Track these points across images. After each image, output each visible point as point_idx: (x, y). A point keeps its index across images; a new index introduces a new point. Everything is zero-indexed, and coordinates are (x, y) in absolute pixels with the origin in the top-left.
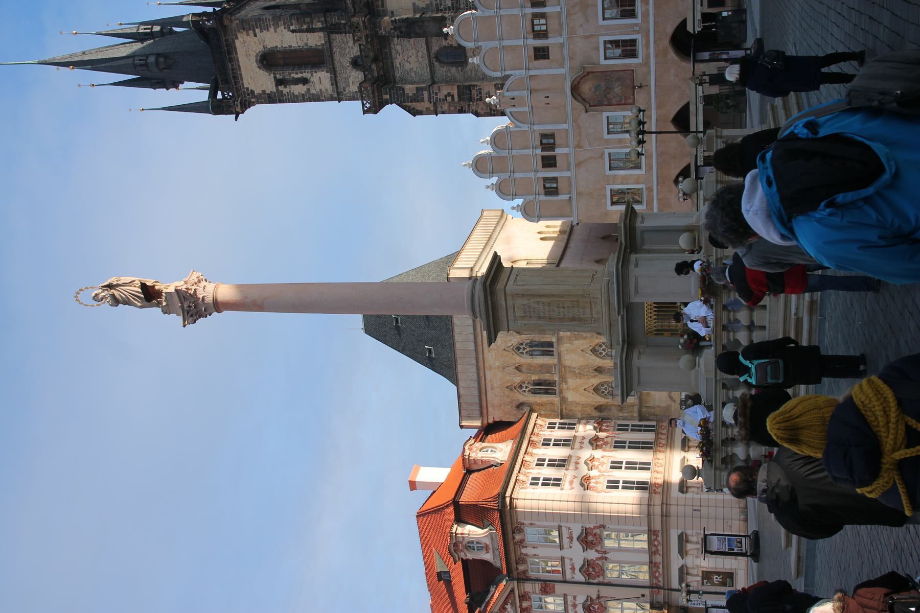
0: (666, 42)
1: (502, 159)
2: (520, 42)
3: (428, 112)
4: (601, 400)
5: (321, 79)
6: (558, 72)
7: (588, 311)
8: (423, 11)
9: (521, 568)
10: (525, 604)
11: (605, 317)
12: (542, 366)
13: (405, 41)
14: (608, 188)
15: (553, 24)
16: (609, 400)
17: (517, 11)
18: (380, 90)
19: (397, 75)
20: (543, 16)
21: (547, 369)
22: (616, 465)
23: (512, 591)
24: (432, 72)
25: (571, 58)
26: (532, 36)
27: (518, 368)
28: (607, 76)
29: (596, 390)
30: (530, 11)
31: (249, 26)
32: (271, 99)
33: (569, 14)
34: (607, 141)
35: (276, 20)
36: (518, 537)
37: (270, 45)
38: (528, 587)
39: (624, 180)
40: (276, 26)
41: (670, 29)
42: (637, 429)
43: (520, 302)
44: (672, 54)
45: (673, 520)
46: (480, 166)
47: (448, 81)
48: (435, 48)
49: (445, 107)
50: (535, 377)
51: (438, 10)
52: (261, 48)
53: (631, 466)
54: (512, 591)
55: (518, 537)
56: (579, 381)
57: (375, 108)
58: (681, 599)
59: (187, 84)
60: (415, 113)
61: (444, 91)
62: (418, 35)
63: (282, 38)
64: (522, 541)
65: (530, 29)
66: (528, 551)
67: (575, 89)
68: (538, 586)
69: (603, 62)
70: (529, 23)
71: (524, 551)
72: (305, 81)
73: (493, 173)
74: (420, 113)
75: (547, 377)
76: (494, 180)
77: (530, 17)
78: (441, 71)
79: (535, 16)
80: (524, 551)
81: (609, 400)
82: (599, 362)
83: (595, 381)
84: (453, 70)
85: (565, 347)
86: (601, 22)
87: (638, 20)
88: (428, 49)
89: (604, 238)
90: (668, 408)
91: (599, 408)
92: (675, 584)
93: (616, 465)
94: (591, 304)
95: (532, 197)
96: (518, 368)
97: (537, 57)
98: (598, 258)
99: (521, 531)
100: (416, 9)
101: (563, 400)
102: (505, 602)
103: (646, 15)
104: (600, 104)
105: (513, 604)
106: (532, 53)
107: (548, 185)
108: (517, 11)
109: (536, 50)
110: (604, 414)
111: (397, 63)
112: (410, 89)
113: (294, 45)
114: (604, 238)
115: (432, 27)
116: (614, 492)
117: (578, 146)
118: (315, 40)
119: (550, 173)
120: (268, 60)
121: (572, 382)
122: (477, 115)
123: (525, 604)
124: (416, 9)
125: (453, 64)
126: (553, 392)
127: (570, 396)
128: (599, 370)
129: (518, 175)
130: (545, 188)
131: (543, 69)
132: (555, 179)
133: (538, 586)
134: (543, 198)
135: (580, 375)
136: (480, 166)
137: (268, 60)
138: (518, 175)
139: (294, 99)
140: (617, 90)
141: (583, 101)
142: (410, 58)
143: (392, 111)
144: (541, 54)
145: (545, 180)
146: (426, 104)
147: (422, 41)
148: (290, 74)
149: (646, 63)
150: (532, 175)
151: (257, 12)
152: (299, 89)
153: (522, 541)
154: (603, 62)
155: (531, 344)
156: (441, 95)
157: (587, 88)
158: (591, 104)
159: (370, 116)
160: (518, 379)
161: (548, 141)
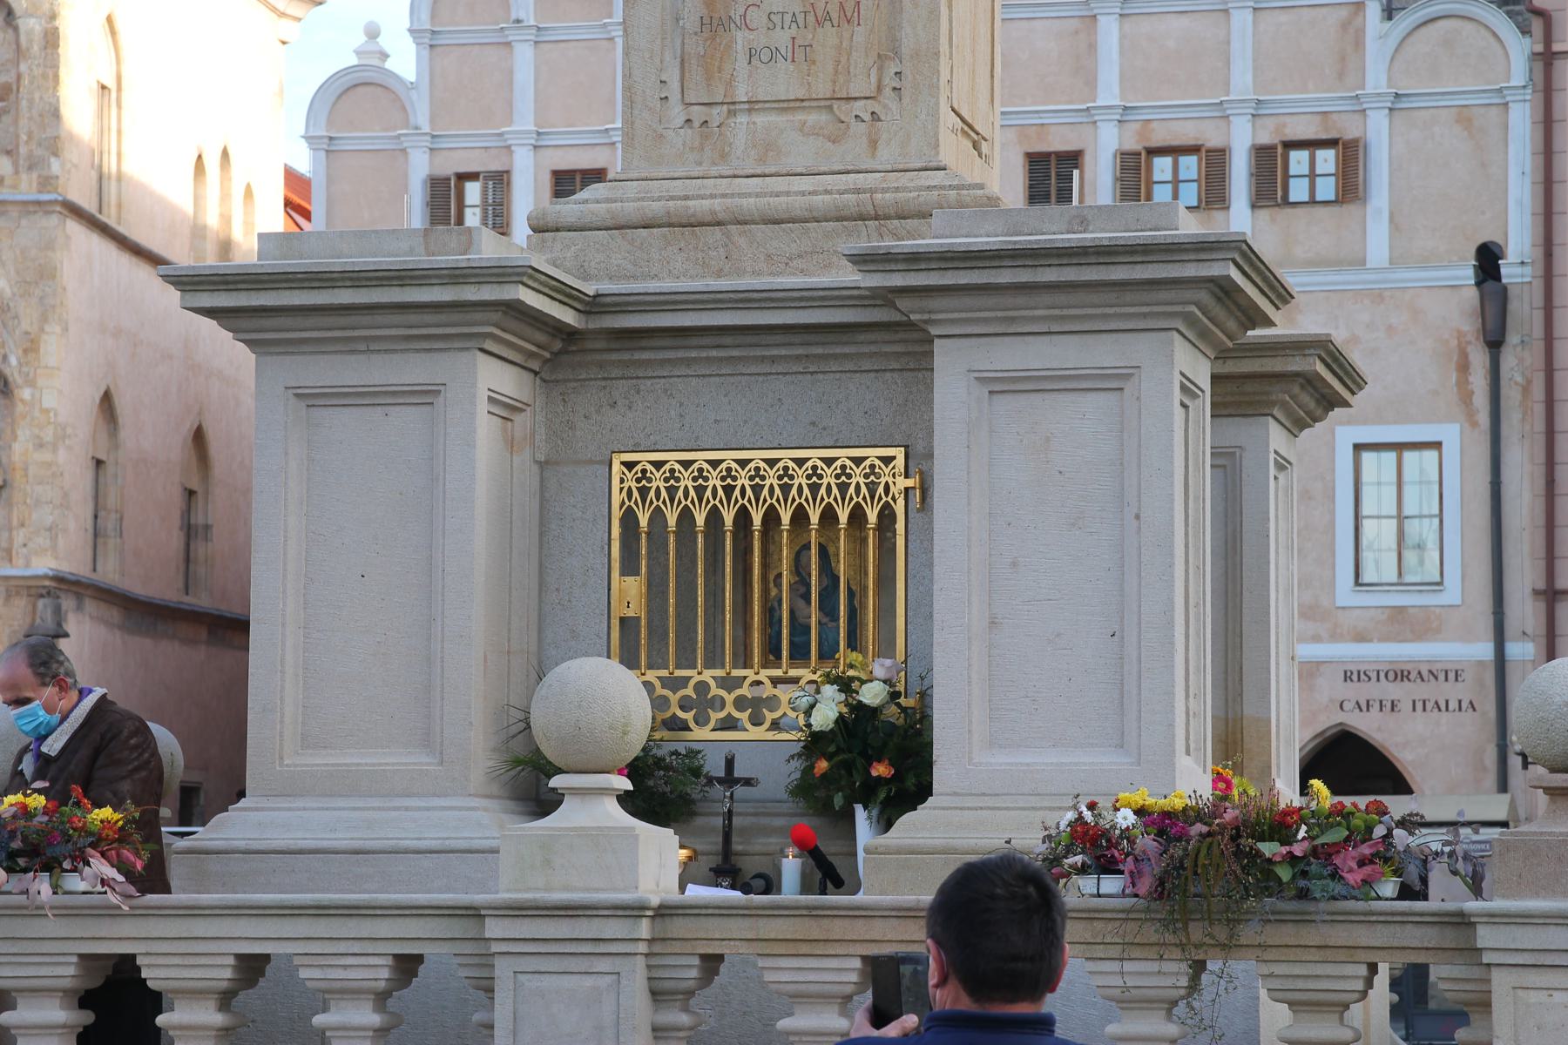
2: (1109, 94)
7: (782, 82)
11: (751, 196)
17: (1242, 82)
26: (1132, 145)
30: (1241, 141)
65: (1160, 138)
70: (1185, 133)
77: (1213, 140)
79: (1215, 162)
89: (199, 437)
94: (829, 103)
95: (422, 118)
97: (1037, 162)
98: (122, 405)
106: (1058, 143)
107: (473, 191)
108: (1242, 82)
114: (199, 437)
129: (524, 57)
130: (463, 177)
134: (420, 167)
138: (524, 57)
145: (500, 181)
150: (524, 121)
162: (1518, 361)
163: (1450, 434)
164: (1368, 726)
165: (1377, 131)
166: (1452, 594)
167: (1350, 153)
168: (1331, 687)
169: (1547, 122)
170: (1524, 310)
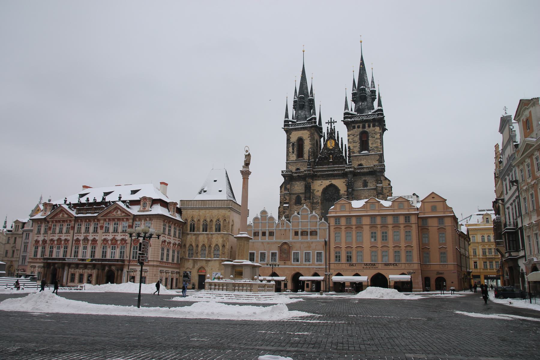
0: (297, 271)
1: (266, 220)
3: (281, 192)
4: (187, 246)
5: (293, 157)
6: (291, 239)
8: (313, 193)
9: (137, 219)
10: (125, 220)
12: (199, 228)
13: (304, 186)
14: (255, 252)
15: (304, 237)
16: (187, 249)
18: (289, 178)
19: (293, 182)
20: (307, 235)
21: (198, 230)
22: (168, 250)
23: (130, 216)
24: (293, 194)
25: (294, 242)
27: (199, 220)
28: (289, 253)
29: (191, 245)
31: (312, 136)
32: (288, 140)
33: (307, 242)
34: (269, 252)
35: (313, 144)
36: (148, 219)
37: (305, 142)
38: (131, 221)
39: (257, 256)
40: (311, 144)
41: (301, 272)
42: (178, 257)
43: (243, 244)
44: (294, 272)
45: (152, 268)
46: (264, 212)
47: (290, 199)
48: (301, 195)
49: (282, 197)
50: (196, 225)
51: (313, 197)
52: (304, 138)
53: (168, 255)
54: (130, 216)
55: (148, 219)
56: (194, 239)
57: (284, 175)
58: (125, 270)
59: (294, 112)
60: (281, 187)
61: (287, 198)
62: (305, 190)
63: (307, 146)
64: (146, 220)
66: (143, 222)
67: (285, 243)
68: (131, 224)
69: (293, 252)
71: (143, 221)
72: (293, 152)
73: (261, 216)
74: (281, 189)
75: (196, 229)
76: (259, 217)
78: (294, 197)
80: (143, 221)
81: (187, 249)
82: (200, 246)
83: (194, 245)
84: (294, 201)
85: (206, 236)
86: (304, 252)
87: (304, 263)
88: (301, 193)
90: (184, 267)
91: (185, 245)
92: (130, 267)
93: (168, 250)
96: (199, 220)
99: (150, 220)
100: (314, 190)
101: (188, 234)
102: (125, 213)
103: (305, 265)
104: (280, 250)
105: (125, 216)
109: (298, 232)
110: (183, 247)
111: (297, 183)
112: (288, 186)
113: (305, 150)
115: (308, 195)
116: (160, 250)
117: (268, 243)
118: (306, 156)
119: (260, 234)
120: (300, 141)
121: (194, 237)
122: (279, 208)
123: (125, 220)
124: (314, 190)
125: (296, 201)
126: (191, 231)
127: (189, 236)
128: (197, 246)
131: (292, 234)
132: (258, 236)
133: (131, 224)
135: (196, 240)
136: (264, 212)
137: (300, 141)
139: (288, 148)
140: (284, 256)
141: (282, 245)
142: (299, 187)
143: (282, 180)
144: (296, 233)
145: (259, 232)
146: (284, 192)
147: (303, 192)
148: (296, 148)
149: (292, 265)
151: (316, 138)
152: (291, 149)
153: (146, 220)
154: (293, 252)
155: (206, 225)
156: (286, 196)
157: (285, 247)
158: (281, 248)
159: (281, 173)
160: (195, 220)
161: (271, 234)
162: (327, 247)
163: (323, 252)
164: (317, 272)
165: (318, 231)
166: (323, 263)
167: (316, 232)
168: (315, 269)
169: (329, 230)
170: (328, 243)
